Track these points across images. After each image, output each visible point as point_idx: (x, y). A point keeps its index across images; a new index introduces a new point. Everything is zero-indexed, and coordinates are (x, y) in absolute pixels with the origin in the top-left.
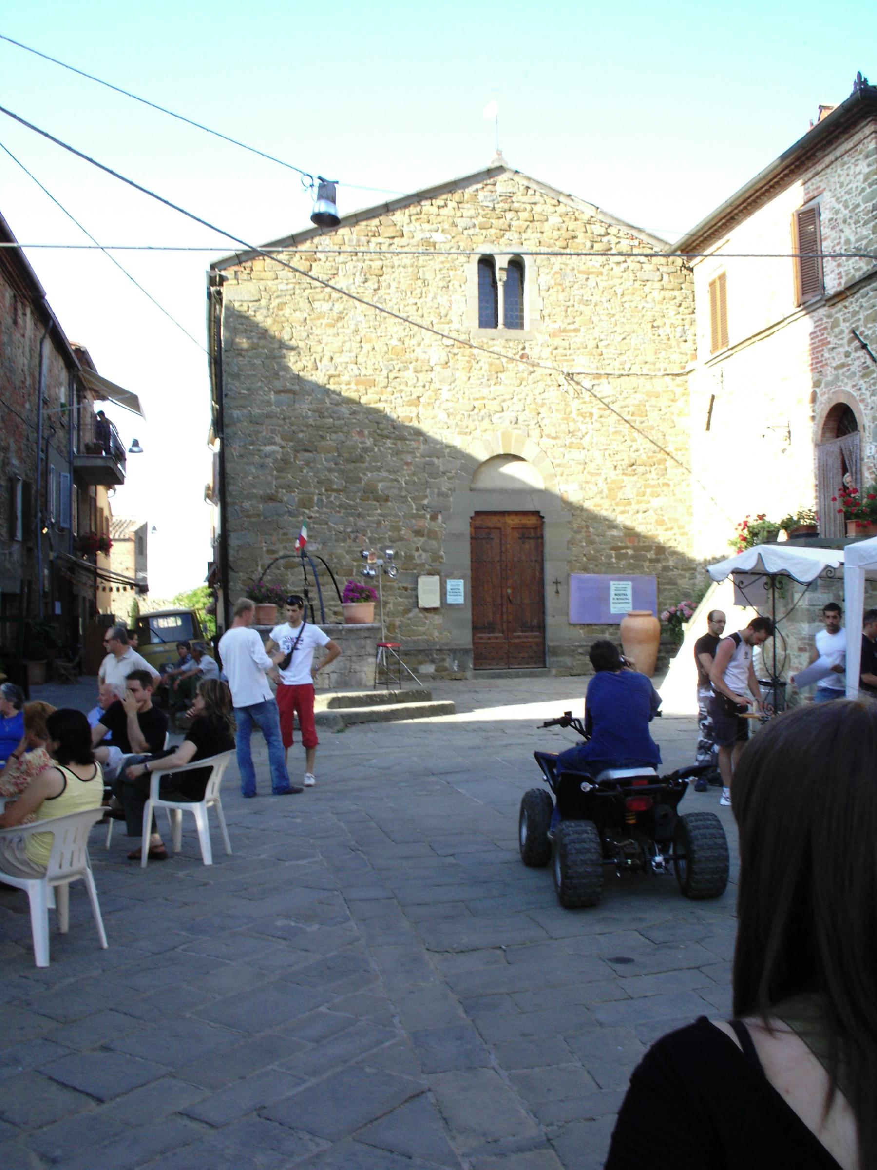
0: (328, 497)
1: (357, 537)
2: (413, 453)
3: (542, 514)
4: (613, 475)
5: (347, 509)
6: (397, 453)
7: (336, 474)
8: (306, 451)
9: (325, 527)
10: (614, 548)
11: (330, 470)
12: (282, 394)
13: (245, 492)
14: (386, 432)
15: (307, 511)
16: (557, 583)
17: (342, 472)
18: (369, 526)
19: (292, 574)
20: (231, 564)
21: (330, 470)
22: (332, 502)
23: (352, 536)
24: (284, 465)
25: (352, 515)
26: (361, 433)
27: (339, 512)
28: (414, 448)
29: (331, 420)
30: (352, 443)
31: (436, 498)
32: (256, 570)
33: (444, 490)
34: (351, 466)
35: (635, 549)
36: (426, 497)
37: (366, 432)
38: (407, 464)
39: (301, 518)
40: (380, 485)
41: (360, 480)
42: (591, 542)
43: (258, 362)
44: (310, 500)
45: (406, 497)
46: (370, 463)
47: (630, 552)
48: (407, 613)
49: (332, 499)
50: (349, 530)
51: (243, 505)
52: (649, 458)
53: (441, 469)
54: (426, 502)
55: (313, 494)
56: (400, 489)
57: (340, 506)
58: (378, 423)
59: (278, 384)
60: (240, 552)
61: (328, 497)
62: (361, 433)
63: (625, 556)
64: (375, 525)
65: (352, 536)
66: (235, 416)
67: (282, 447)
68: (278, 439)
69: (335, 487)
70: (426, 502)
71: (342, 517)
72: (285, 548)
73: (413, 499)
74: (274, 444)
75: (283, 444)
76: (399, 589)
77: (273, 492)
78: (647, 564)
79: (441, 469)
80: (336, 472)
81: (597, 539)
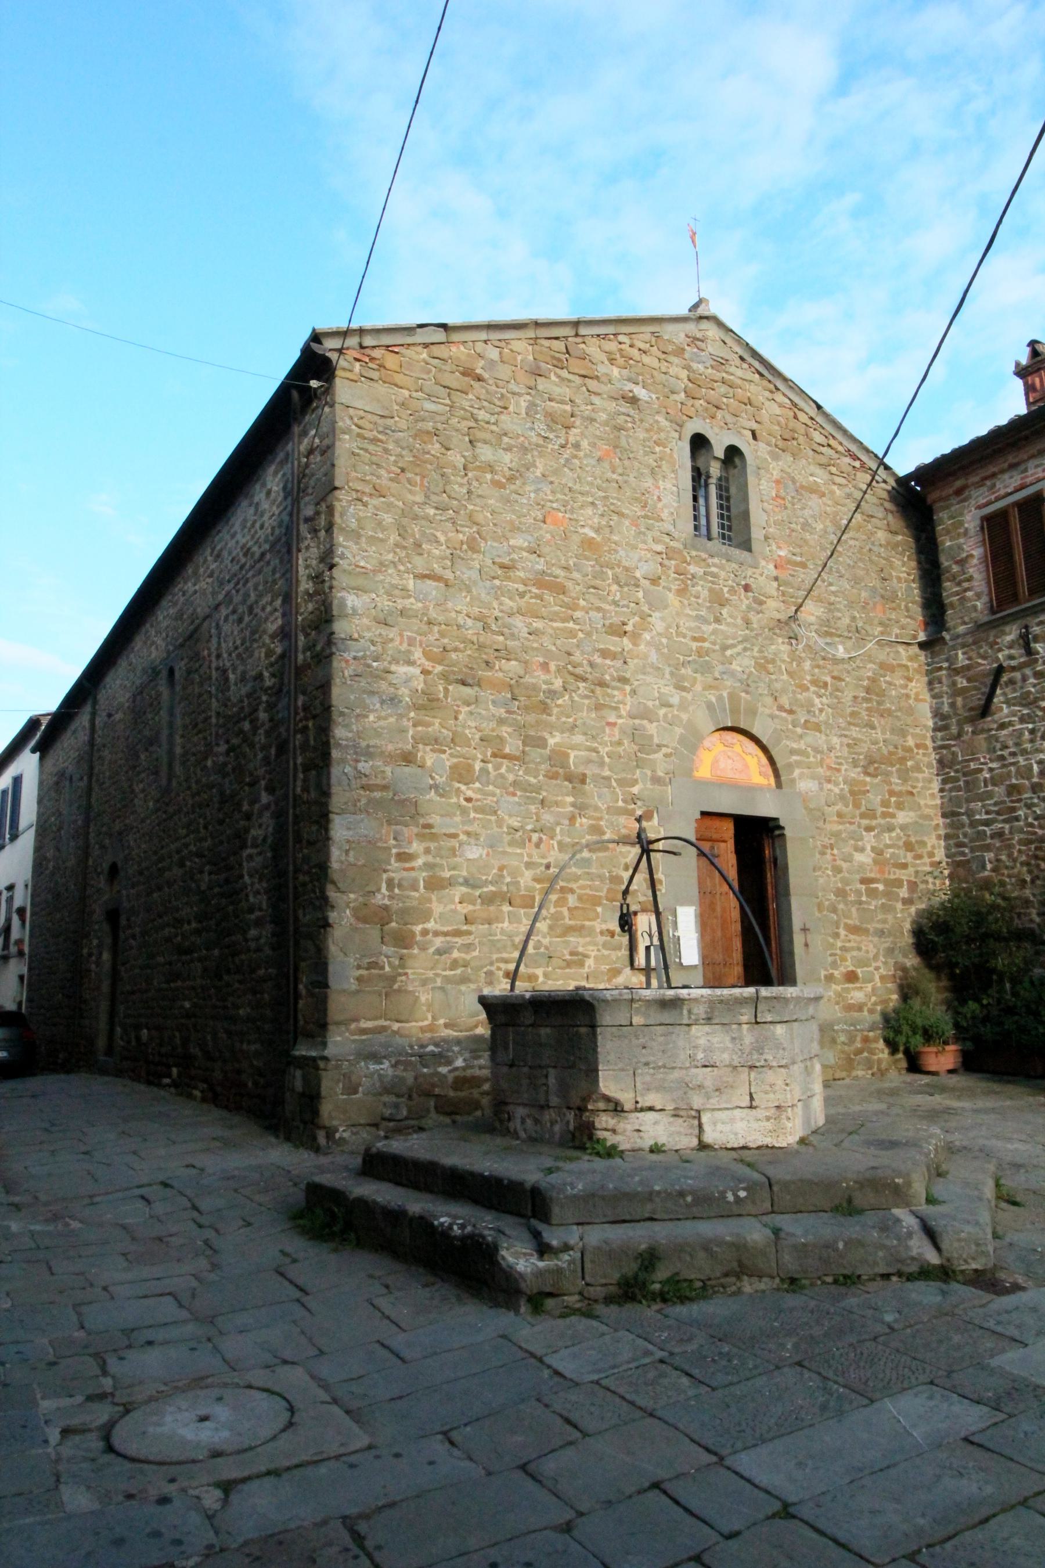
0: (497, 768)
1: (541, 839)
2: (616, 709)
3: (782, 823)
4: (855, 774)
5: (525, 790)
6: (599, 707)
7: (509, 730)
8: (464, 683)
9: (493, 818)
10: (864, 881)
11: (501, 721)
12: (429, 582)
13: (364, 744)
14: (579, 671)
15: (463, 788)
16: (805, 930)
17: (520, 728)
18: (558, 824)
19: (439, 901)
20: (335, 876)
21: (501, 721)
22: (502, 776)
23: (535, 837)
24: (428, 703)
25: (532, 800)
26: (545, 666)
27: (514, 795)
28: (619, 702)
29: (501, 638)
30: (534, 681)
31: (649, 785)
32: (379, 890)
33: (660, 774)
34: (531, 718)
35: (888, 883)
36: (636, 782)
37: (553, 667)
38: (609, 724)
39: (454, 800)
40: (572, 754)
41: (542, 743)
42: (837, 870)
43: (388, 519)
44: (470, 768)
45: (608, 779)
46: (558, 719)
47: (881, 887)
48: (615, 976)
49: (503, 770)
50: (529, 827)
51: (360, 765)
52: (890, 753)
53: (656, 741)
54: (635, 790)
55: (474, 759)
56: (602, 764)
57: (515, 783)
58: (569, 654)
59: (420, 563)
60: (352, 853)
61: (497, 768)
62: (545, 666)
63: (872, 893)
64: (567, 822)
65: (535, 837)
66: (349, 604)
67: (425, 672)
68: (417, 654)
69: (507, 750)
70: (635, 790)
71: (520, 804)
72: (427, 851)
73: (621, 783)
74: (410, 663)
75: (428, 665)
76: (602, 933)
77: (410, 747)
78: (899, 906)
79: (656, 741)
80: (510, 726)
81: (845, 865)
